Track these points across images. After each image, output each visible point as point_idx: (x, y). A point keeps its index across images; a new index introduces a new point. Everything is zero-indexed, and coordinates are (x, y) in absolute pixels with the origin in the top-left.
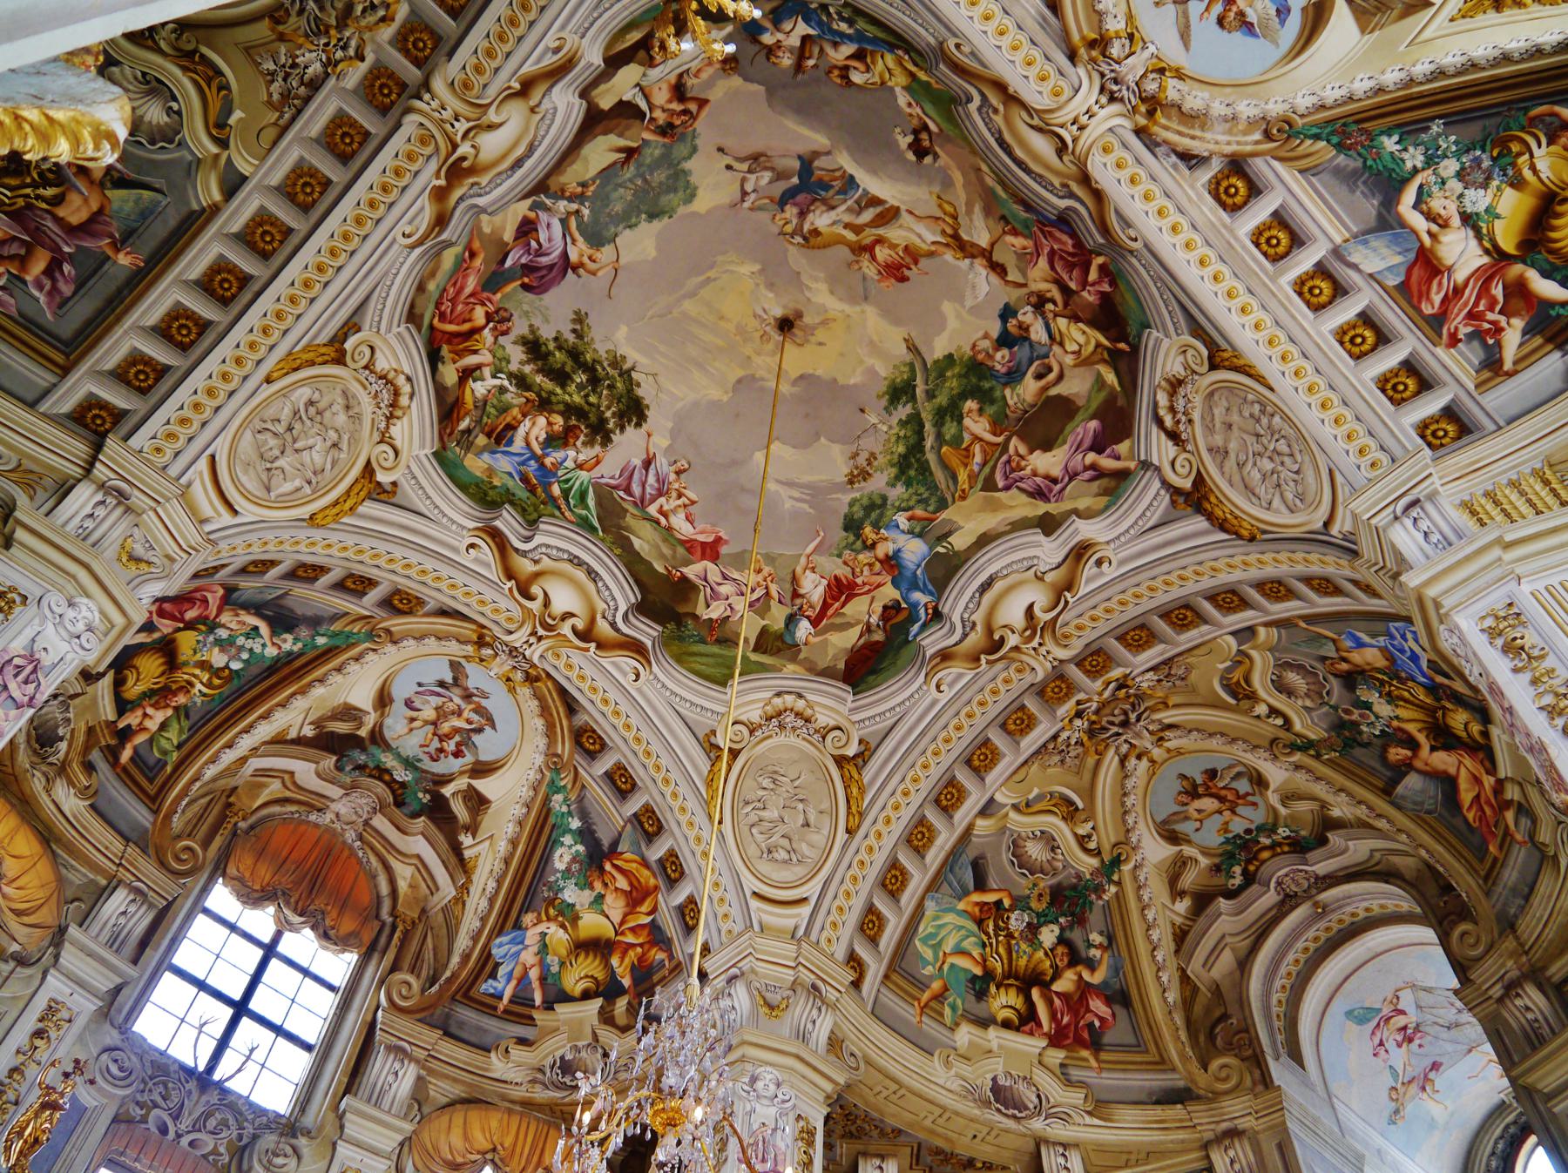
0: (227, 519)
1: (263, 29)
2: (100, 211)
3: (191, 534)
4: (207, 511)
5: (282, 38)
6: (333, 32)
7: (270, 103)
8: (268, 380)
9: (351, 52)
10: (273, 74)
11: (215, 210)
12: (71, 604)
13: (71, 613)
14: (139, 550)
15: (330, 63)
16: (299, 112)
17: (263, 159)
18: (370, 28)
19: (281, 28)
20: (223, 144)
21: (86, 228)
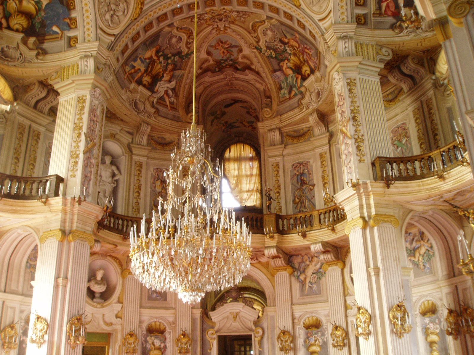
0: (332, 15)
1: (237, 23)
2: (292, 39)
3: (331, 31)
4: (329, 23)
5: (235, 20)
6: (225, 14)
7: (249, 16)
8: (299, 7)
9: (225, 10)
10: (244, 18)
11: (276, 20)
12: (335, 79)
13: (336, 80)
14: (334, 48)
15: (231, 12)
16: (245, 12)
17: (260, 14)
18: (217, 11)
19: (234, 21)
20: (264, 21)
21: (297, 42)
